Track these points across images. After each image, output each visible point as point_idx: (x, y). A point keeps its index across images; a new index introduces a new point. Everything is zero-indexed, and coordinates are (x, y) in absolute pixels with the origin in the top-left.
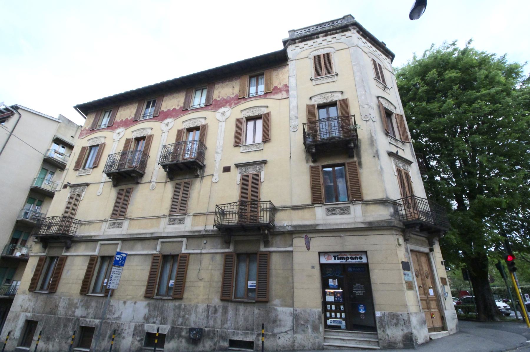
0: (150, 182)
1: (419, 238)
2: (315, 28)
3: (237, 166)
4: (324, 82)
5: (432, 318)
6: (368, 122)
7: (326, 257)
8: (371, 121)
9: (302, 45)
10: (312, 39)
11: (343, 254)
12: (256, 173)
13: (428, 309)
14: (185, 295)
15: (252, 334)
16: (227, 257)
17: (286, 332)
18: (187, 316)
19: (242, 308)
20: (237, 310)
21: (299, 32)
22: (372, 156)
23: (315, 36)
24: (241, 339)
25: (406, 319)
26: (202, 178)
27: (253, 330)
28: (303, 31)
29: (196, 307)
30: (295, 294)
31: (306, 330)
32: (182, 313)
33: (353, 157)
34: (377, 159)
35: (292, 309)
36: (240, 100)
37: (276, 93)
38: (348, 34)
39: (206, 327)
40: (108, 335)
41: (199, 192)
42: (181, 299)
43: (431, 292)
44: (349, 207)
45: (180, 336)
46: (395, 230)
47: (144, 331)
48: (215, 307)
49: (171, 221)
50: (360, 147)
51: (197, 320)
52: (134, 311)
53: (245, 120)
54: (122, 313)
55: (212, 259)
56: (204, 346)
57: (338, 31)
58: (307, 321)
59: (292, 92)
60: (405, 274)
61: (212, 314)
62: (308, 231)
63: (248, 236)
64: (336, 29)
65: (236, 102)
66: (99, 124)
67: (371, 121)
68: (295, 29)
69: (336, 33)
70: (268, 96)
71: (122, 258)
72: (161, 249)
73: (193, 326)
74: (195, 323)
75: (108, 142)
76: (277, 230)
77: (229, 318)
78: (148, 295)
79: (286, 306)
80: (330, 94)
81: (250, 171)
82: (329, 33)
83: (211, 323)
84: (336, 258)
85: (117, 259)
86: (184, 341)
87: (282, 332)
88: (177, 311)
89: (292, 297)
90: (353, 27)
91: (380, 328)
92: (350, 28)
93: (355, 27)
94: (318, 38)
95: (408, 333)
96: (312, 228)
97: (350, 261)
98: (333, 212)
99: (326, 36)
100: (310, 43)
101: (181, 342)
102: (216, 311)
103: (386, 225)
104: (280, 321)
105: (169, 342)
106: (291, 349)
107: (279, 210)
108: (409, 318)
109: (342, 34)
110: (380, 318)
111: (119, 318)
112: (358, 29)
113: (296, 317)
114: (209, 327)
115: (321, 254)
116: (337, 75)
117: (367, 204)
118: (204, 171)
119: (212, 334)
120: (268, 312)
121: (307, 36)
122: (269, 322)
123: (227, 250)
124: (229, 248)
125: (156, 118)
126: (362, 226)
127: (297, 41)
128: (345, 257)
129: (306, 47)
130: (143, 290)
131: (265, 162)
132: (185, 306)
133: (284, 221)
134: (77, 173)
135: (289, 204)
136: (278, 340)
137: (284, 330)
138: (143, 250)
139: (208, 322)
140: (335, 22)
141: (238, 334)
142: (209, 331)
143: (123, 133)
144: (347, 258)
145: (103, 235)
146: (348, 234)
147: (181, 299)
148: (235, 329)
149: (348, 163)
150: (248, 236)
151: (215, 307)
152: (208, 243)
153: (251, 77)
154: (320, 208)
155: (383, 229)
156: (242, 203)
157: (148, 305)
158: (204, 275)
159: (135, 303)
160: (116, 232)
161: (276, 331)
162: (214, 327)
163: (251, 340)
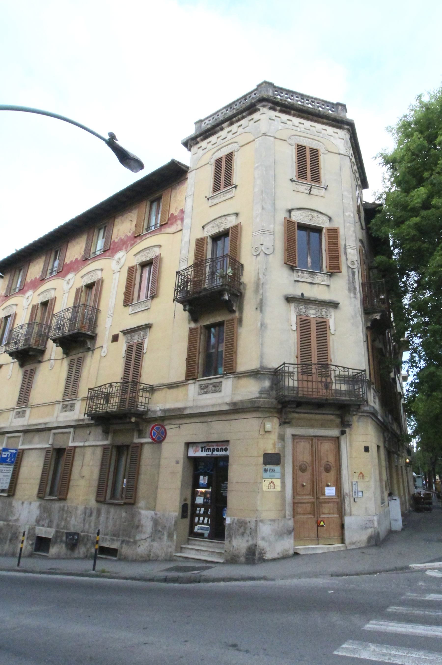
0: (50, 360)
2: (243, 101)
3: (126, 332)
6: (259, 258)
7: (194, 448)
9: (204, 144)
10: (215, 133)
11: (210, 444)
12: (141, 341)
14: (69, 496)
15: (117, 540)
16: (105, 449)
17: (145, 539)
18: (68, 519)
19: (112, 510)
20: (108, 512)
22: (254, 308)
23: (218, 128)
24: (108, 546)
25: (253, 527)
26: (93, 351)
27: (118, 536)
28: (211, 118)
29: (76, 508)
30: (159, 495)
31: (162, 537)
32: (65, 516)
33: (234, 311)
34: (259, 311)
35: (153, 513)
36: (136, 240)
37: (172, 224)
38: (256, 116)
39: (82, 532)
40: (9, 538)
41: (89, 371)
42: (65, 499)
44: (221, 382)
45: (61, 541)
46: (262, 412)
47: (35, 534)
48: (91, 509)
49: (64, 408)
51: (76, 523)
52: (29, 512)
53: (209, 241)
54: (20, 514)
55: (94, 453)
56: (79, 553)
57: (244, 114)
58: (164, 528)
59: (187, 221)
60: (266, 470)
61: (88, 517)
62: (178, 416)
63: (123, 422)
65: (132, 242)
66: (92, 251)
68: (202, 118)
69: (243, 118)
70: (164, 230)
71: (11, 455)
72: (53, 442)
73: (72, 530)
74: (74, 526)
75: (164, 253)
76: (150, 417)
77: (101, 522)
78: (41, 496)
79: (149, 509)
80: (224, 218)
81: (136, 339)
82: (234, 119)
83: (87, 526)
84: (204, 449)
85: (3, 456)
86: (64, 546)
87: (142, 540)
88: (61, 512)
89: (155, 499)
90: (261, 104)
91: (227, 538)
92: (258, 106)
93: (264, 103)
94: (222, 129)
95: (252, 545)
96: (179, 413)
97: (215, 453)
98: (205, 390)
99: (231, 124)
100: (213, 139)
101: (62, 547)
102: (91, 515)
103: (249, 406)
104: (142, 526)
105: (53, 547)
106: (148, 559)
107: (156, 390)
108: (256, 526)
109: (250, 117)
110: (229, 525)
111: (17, 520)
112: (270, 105)
113: (156, 522)
114: (84, 532)
115: (190, 445)
116: (236, 187)
117: (239, 378)
118: (95, 342)
119: (86, 540)
120: (133, 516)
122: (133, 527)
123: (105, 443)
124: (107, 440)
125: (60, 274)
126: (226, 408)
127: (198, 139)
128: (212, 448)
129: (209, 146)
130: (35, 491)
131: (148, 326)
132: (68, 508)
133: (160, 403)
134: (130, 310)
135: (166, 382)
136: (137, 548)
137: (144, 536)
138: (39, 443)
139: (84, 526)
140: (248, 97)
141: (106, 539)
142: (84, 536)
143: (124, 258)
144: (213, 450)
145: (10, 427)
146: (215, 418)
147: (65, 499)
148: (105, 535)
149: (227, 321)
150: (123, 422)
151: (91, 509)
152: (92, 434)
153: (152, 202)
154: (193, 385)
155: (247, 412)
156: (125, 382)
157: (40, 506)
158: (86, 472)
159: (30, 503)
160: (19, 423)
161: (137, 538)
162: (88, 532)
163: (116, 548)
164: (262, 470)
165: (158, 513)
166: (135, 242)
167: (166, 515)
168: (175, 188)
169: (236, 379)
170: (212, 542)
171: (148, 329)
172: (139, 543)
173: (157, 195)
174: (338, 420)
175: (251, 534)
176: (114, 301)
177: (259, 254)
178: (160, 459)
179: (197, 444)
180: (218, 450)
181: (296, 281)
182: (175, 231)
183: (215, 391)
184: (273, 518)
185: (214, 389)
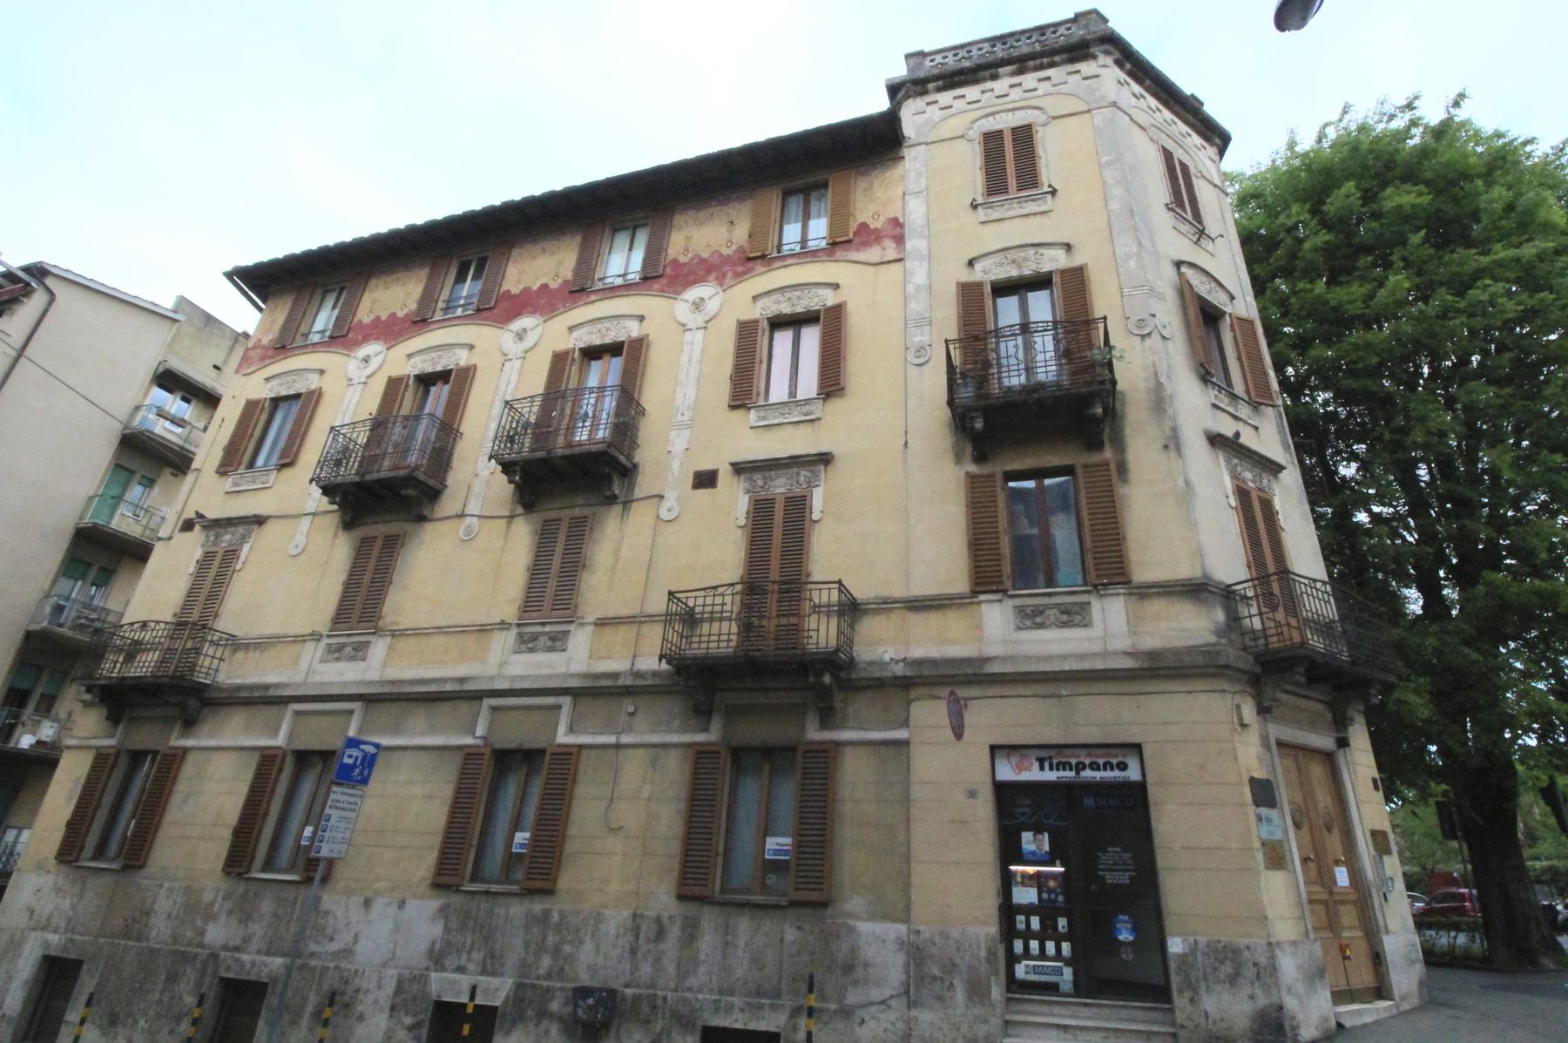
0: (462, 516)
1: (1303, 703)
2: (986, 46)
3: (739, 469)
4: (1011, 213)
5: (1345, 958)
6: (1148, 342)
7: (1014, 760)
8: (1156, 336)
9: (945, 98)
10: (976, 81)
11: (1068, 752)
12: (798, 491)
13: (1332, 930)
14: (565, 880)
15: (774, 1007)
16: (701, 757)
17: (883, 1002)
18: (567, 948)
19: (744, 925)
21: (939, 58)
23: (987, 73)
24: (739, 1026)
25: (1263, 960)
26: (627, 504)
27: (777, 994)
28: (950, 54)
29: (599, 919)
30: (915, 880)
31: (947, 995)
32: (551, 940)
34: (1173, 454)
35: (903, 928)
36: (750, 264)
37: (866, 244)
38: (1087, 67)
39: (627, 985)
41: (617, 552)
42: (550, 892)
43: (1342, 876)
46: (1230, 679)
48: (658, 920)
49: (523, 642)
50: (1122, 418)
51: (600, 960)
55: (654, 763)
57: (1057, 59)
58: (951, 967)
60: (1259, 819)
61: (649, 941)
62: (959, 679)
63: (768, 691)
64: (1054, 52)
65: (739, 269)
67: (1156, 336)
68: (926, 50)
69: (1052, 65)
70: (839, 254)
72: (489, 731)
73: (585, 979)
74: (591, 968)
76: (863, 675)
77: (703, 957)
78: (445, 878)
79: (885, 917)
80: (1031, 252)
81: (780, 486)
82: (1031, 63)
83: (646, 970)
84: (1046, 765)
85: (347, 760)
87: (871, 1004)
89: (906, 887)
91: (1180, 992)
94: (994, 77)
95: (1271, 1006)
96: (969, 670)
97: (1087, 774)
98: (1038, 620)
99: (1020, 72)
100: (971, 92)
102: (660, 934)
104: (866, 965)
107: (866, 612)
108: (1273, 957)
109: (1071, 68)
110: (1183, 958)
112: (1117, 55)
113: (915, 953)
114: (638, 986)
115: (997, 752)
116: (1053, 192)
118: (631, 487)
119: (645, 1009)
121: (961, 72)
124: (706, 730)
125: (485, 314)
126: (1129, 663)
127: (931, 86)
128: (1074, 761)
131: (825, 459)
133: (885, 644)
135: (898, 592)
136: (857, 1029)
137: (876, 994)
139: (634, 970)
142: (636, 998)
144: (1080, 767)
145: (305, 683)
146: (1082, 689)
147: (550, 892)
148: (721, 992)
149: (1085, 466)
151: (658, 920)
153: (787, 194)
156: (752, 587)
158: (629, 815)
161: (852, 998)
163: (773, 1029)
164: (1253, 819)
165: (922, 928)
166: (750, 270)
167: (955, 934)
168: (866, 173)
169: (1133, 598)
170: (1086, 1005)
171: (822, 467)
172: (859, 1013)
173: (819, 177)
174: (1329, 716)
175: (1258, 978)
176: (691, 393)
177: (1149, 334)
178: (907, 785)
179: (1023, 752)
180: (1095, 766)
181: (1214, 406)
182: (877, 260)
183: (550, 649)
184: (1293, 938)
185: (549, 643)
